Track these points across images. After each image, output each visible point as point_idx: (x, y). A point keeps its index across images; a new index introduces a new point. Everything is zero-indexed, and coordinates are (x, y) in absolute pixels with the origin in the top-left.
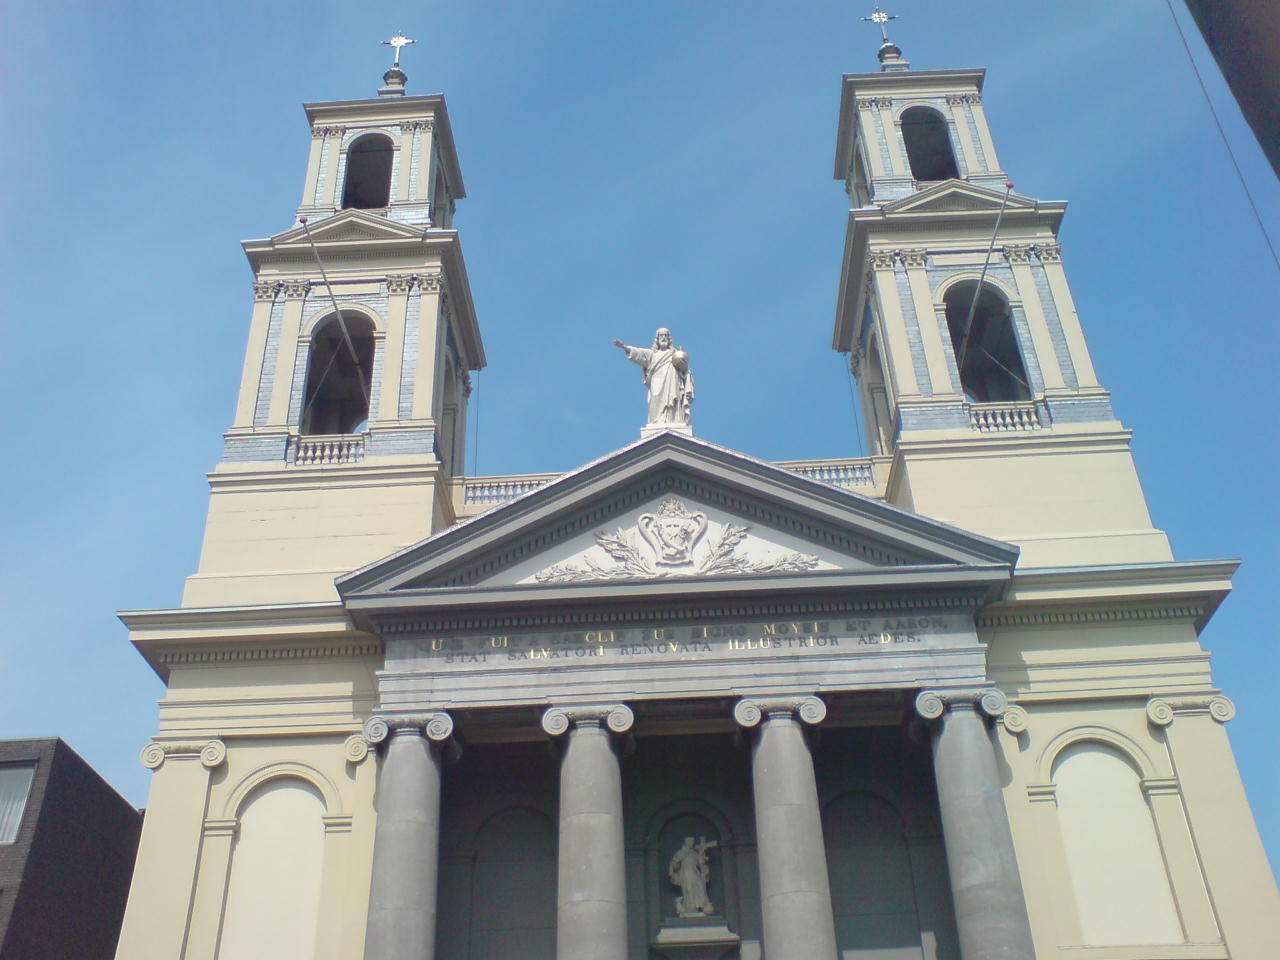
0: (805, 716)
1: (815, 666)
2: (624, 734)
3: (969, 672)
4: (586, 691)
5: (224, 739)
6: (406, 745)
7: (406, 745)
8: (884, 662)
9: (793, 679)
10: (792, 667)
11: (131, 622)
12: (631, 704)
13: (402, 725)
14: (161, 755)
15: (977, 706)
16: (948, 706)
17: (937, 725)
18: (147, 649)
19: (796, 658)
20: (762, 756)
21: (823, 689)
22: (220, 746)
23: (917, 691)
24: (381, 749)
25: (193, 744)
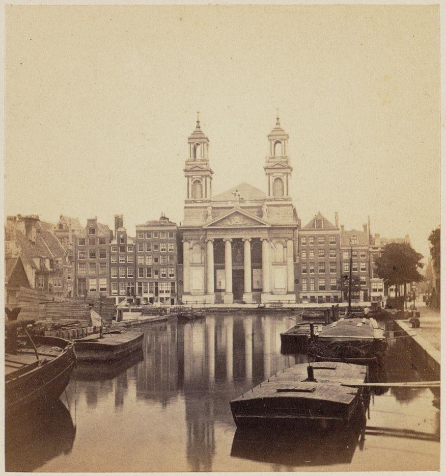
4: (228, 237)
23: (260, 238)
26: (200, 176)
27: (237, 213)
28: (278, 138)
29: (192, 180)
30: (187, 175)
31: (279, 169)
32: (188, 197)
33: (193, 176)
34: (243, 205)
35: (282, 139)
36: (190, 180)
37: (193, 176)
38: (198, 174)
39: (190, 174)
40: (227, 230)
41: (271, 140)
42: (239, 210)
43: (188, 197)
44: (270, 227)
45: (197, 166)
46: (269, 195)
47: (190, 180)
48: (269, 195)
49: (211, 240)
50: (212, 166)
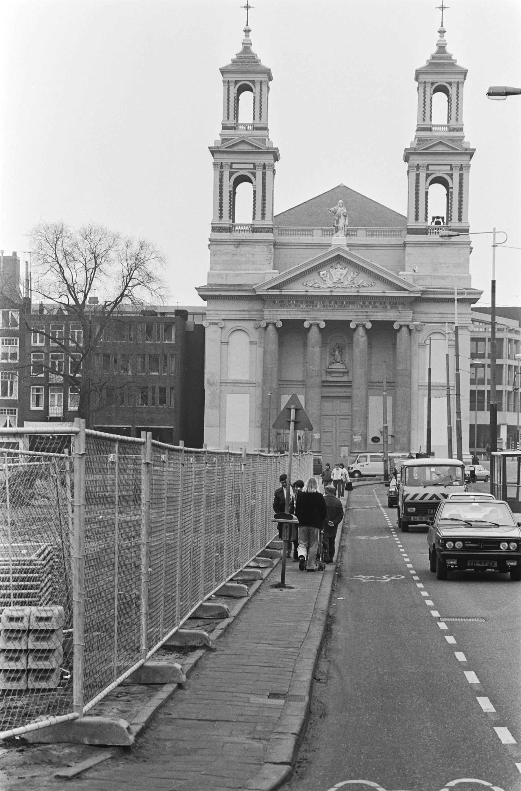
0: (366, 327)
1: (371, 314)
2: (322, 329)
3: (408, 317)
5: (223, 320)
6: (271, 327)
7: (271, 327)
8: (388, 314)
9: (365, 317)
10: (365, 314)
11: (196, 288)
12: (324, 321)
13: (270, 323)
14: (208, 324)
15: (408, 326)
16: (401, 326)
17: (399, 330)
18: (201, 296)
19: (367, 312)
20: (356, 336)
21: (372, 320)
22: (222, 322)
24: (266, 328)
25: (216, 321)
26: (251, 166)
27: (338, 259)
28: (442, 80)
29: (231, 174)
30: (219, 161)
31: (440, 159)
32: (221, 217)
33: (234, 166)
34: (354, 240)
35: (450, 84)
36: (226, 174)
37: (234, 166)
38: (244, 158)
39: (226, 159)
40: (310, 300)
41: (425, 82)
42: (344, 251)
43: (221, 217)
44: (419, 295)
45: (243, 142)
46: (417, 219)
47: (226, 174)
48: (417, 219)
49: (274, 324)
50: (275, 138)
